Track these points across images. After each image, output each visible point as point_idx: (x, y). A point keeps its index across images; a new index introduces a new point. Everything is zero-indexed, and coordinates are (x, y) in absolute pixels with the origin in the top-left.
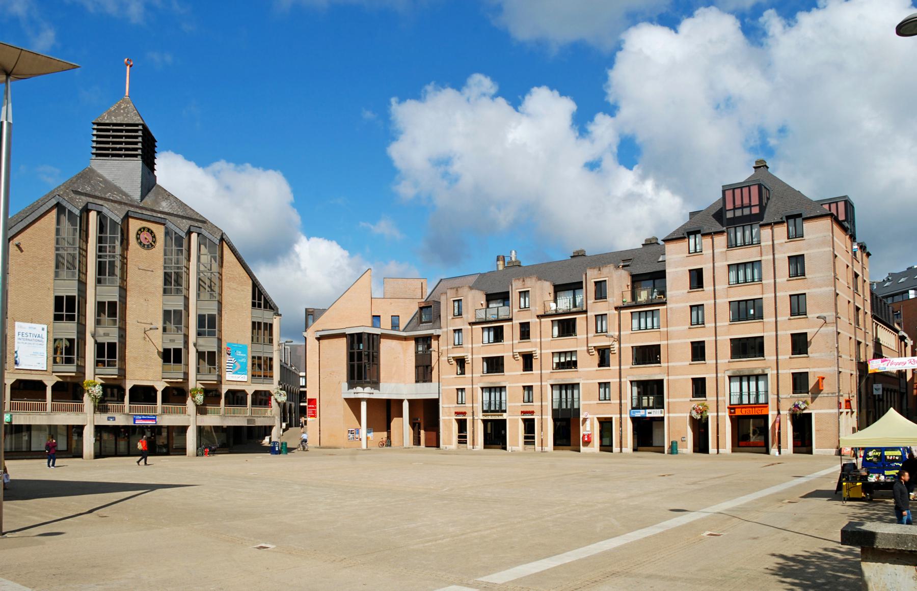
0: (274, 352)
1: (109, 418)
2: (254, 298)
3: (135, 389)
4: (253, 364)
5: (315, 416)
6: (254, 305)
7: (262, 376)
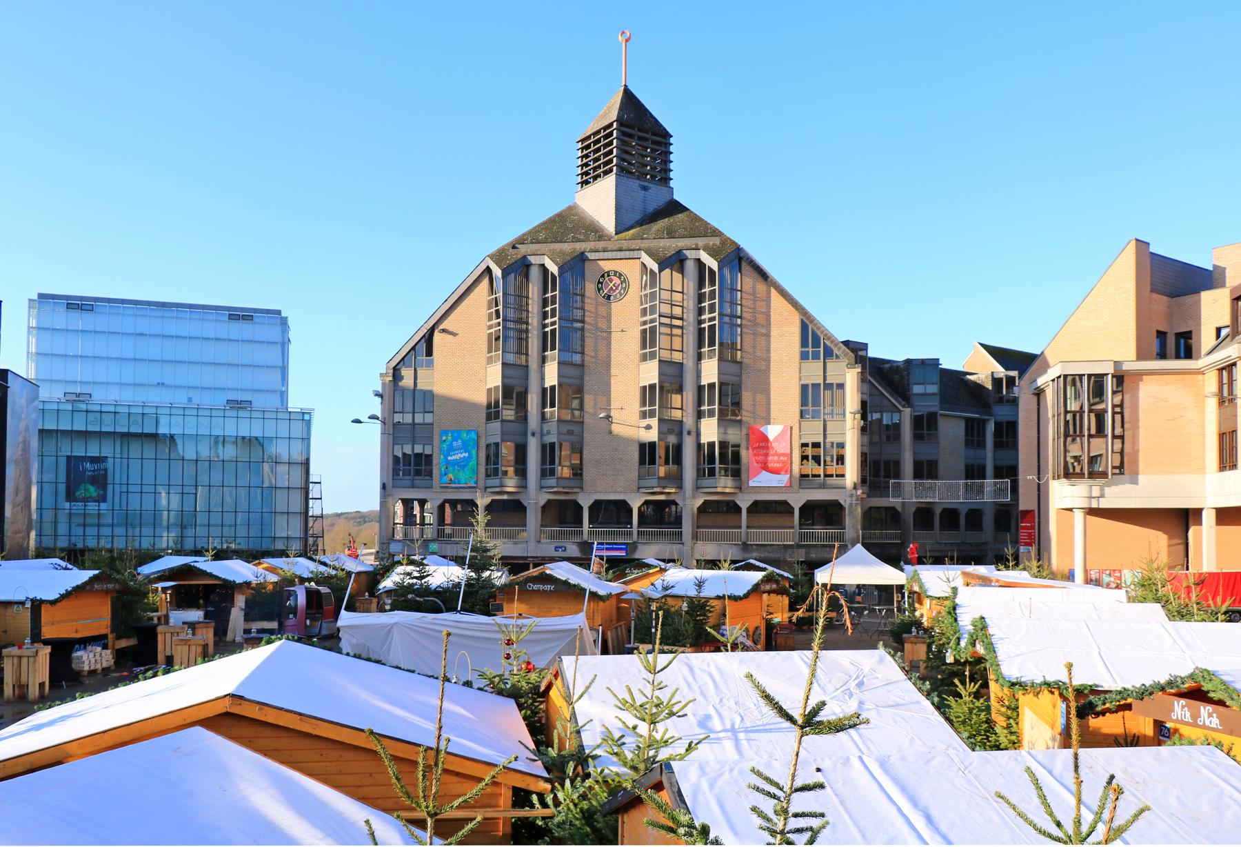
0: (847, 432)
1: (557, 549)
2: (804, 343)
3: (597, 506)
4: (804, 458)
5: (1030, 544)
6: (804, 356)
7: (822, 475)
